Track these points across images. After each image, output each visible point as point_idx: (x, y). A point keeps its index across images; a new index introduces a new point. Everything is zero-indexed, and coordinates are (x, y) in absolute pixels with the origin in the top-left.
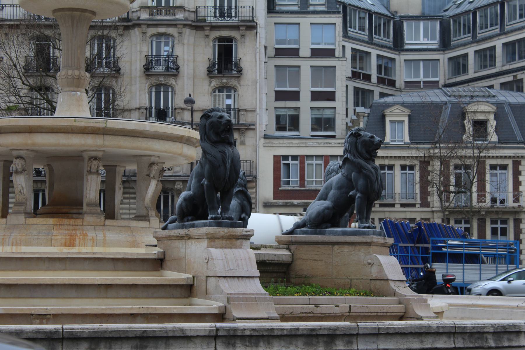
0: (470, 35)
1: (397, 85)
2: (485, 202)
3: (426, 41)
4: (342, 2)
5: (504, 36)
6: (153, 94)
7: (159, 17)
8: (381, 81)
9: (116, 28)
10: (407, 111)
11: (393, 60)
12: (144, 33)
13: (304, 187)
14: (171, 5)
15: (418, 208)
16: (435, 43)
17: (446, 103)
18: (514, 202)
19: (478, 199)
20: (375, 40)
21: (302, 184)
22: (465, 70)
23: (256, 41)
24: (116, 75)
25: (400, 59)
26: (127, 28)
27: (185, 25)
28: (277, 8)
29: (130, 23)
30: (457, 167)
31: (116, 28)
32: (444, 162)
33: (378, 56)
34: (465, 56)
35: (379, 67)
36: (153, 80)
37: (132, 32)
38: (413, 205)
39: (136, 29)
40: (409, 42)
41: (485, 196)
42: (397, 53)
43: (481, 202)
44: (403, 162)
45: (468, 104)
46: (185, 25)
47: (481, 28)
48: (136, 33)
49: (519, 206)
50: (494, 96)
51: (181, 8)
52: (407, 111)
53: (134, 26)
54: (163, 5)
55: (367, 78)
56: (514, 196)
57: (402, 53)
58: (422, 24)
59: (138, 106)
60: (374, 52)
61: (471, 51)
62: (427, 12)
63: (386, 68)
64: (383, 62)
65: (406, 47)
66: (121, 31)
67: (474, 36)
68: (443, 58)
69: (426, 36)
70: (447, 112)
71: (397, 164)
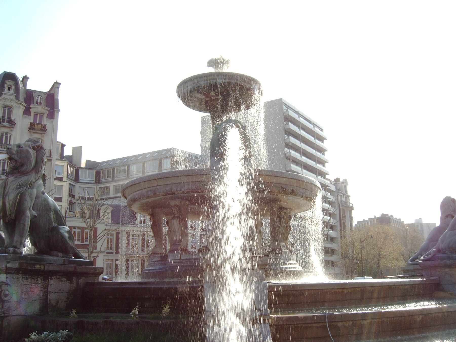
0: (111, 178)
1: (76, 198)
3: (89, 179)
13: (83, 243)
14: (8, 143)
15: (114, 255)
16: (93, 180)
22: (108, 193)
23: (51, 168)
25: (77, 186)
38: (112, 253)
40: (81, 178)
42: (76, 183)
54: (4, 142)
57: (78, 183)
58: (87, 171)
62: (88, 167)
65: (80, 181)
69: (89, 177)
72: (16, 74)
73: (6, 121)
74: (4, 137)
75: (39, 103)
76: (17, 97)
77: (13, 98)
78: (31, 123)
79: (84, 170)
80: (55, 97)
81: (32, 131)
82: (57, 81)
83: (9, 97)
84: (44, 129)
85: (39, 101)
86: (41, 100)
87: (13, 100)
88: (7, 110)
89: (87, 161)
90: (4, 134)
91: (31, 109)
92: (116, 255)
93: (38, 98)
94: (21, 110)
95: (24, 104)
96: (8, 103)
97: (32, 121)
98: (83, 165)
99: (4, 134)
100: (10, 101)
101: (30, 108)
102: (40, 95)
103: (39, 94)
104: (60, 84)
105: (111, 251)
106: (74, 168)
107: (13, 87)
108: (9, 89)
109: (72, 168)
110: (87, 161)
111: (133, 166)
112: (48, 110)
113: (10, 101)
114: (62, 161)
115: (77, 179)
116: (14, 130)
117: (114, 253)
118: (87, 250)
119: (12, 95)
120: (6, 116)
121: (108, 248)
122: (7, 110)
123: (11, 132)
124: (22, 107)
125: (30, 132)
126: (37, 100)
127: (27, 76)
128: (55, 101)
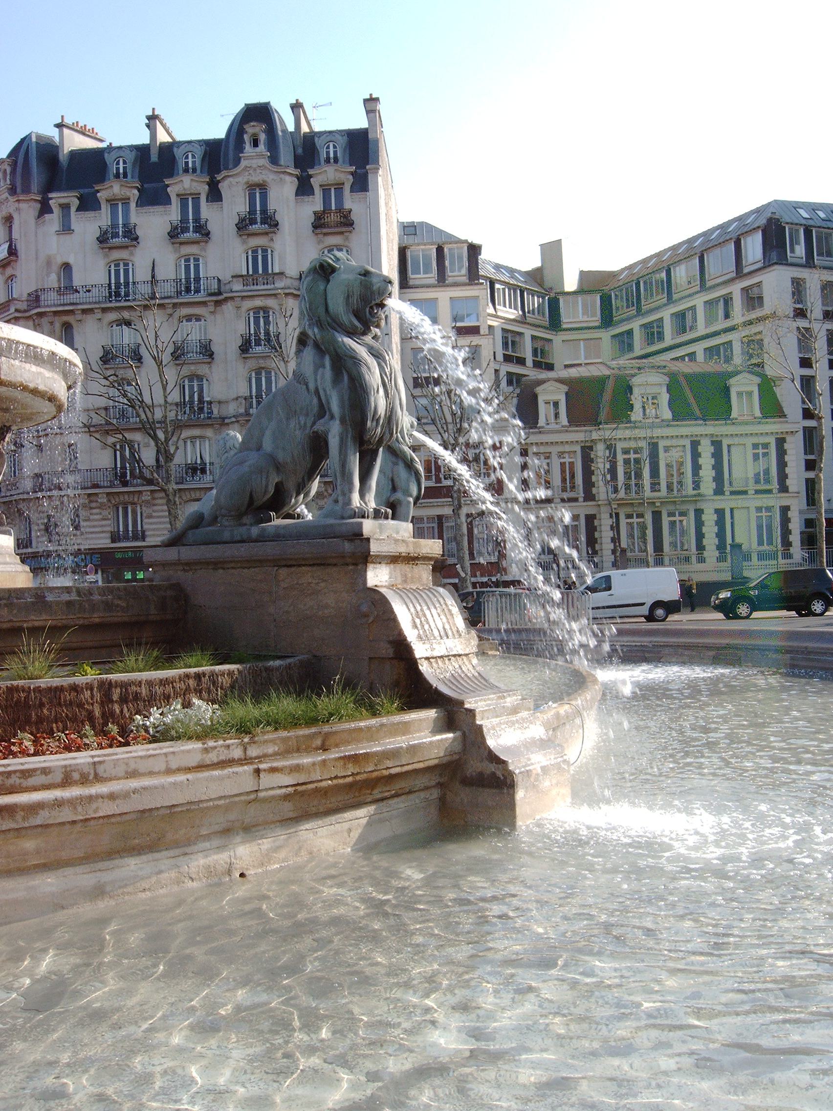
0: (635, 308)
2: (659, 491)
4: (488, 277)
5: (672, 305)
6: (254, 380)
7: (255, 287)
8: (537, 365)
9: (204, 304)
10: (565, 388)
11: (550, 341)
12: (238, 308)
14: (270, 272)
17: (609, 377)
18: (694, 489)
19: (651, 488)
20: (529, 320)
21: (438, 480)
22: (630, 347)
24: (209, 360)
25: (558, 339)
26: (218, 303)
27: (287, 295)
28: (411, 283)
29: (220, 298)
30: (626, 451)
31: (204, 304)
32: (610, 447)
33: (534, 338)
34: (630, 333)
35: (535, 352)
36: (252, 364)
37: (224, 307)
39: (229, 304)
40: (567, 318)
41: (659, 484)
43: (655, 491)
44: (561, 449)
45: (633, 376)
46: (287, 295)
47: (646, 299)
48: (229, 307)
49: (699, 495)
50: (665, 367)
51: (281, 274)
52: (565, 388)
53: (226, 300)
54: (260, 271)
55: (521, 361)
56: (694, 482)
58: (580, 299)
59: (235, 396)
60: (528, 332)
61: (635, 325)
63: (542, 352)
64: (539, 345)
65: (564, 326)
66: (212, 309)
67: (639, 309)
68: (605, 336)
70: (609, 386)
71: (554, 450)
72: (272, 104)
73: (259, 220)
74: (260, 258)
75: (332, 161)
76: (274, 160)
77: (264, 162)
78: (315, 213)
79: (570, 298)
80: (371, 136)
81: (318, 231)
82: (371, 95)
83: (255, 163)
84: (346, 222)
85: (332, 155)
86: (335, 153)
87: (266, 167)
88: (258, 195)
89: (582, 273)
90: (260, 252)
91: (312, 180)
92: (585, 504)
93: (328, 147)
94: (289, 185)
95: (297, 172)
96: (256, 178)
97: (319, 207)
98: (571, 283)
99: (260, 252)
100: (258, 171)
101: (311, 176)
102: (333, 138)
103: (329, 139)
104: (377, 100)
105: (572, 495)
106: (543, 298)
107: (262, 137)
108: (256, 144)
109: (538, 297)
110: (583, 275)
111: (677, 268)
112: (352, 174)
113: (258, 171)
114: (476, 287)
115: (555, 323)
116: (278, 238)
117: (581, 499)
118: (450, 499)
119: (261, 156)
120: (258, 208)
121: (564, 490)
122: (258, 195)
123: (271, 244)
124: (288, 178)
125: (317, 234)
126: (328, 153)
127: (301, 101)
128: (370, 146)
